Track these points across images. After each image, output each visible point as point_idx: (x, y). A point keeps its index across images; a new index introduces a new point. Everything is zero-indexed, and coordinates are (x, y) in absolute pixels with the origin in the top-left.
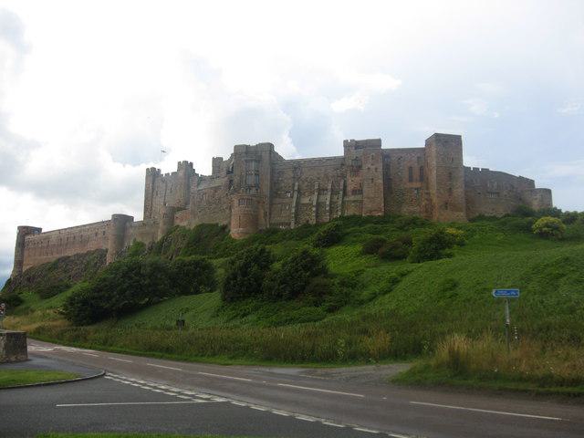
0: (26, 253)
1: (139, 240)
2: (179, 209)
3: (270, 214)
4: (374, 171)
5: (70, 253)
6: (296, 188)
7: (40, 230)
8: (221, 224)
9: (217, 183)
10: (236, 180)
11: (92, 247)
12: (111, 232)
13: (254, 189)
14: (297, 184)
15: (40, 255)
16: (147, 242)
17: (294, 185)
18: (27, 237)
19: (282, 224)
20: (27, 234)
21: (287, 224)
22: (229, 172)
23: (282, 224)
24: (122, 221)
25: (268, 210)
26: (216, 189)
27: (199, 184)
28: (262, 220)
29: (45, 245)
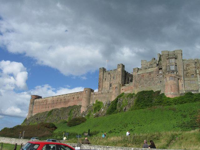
0: (34, 107)
1: (99, 100)
5: (59, 107)
7: (41, 97)
9: (150, 70)
10: (164, 68)
11: (71, 104)
13: (175, 72)
14: (197, 70)
15: (42, 108)
16: (104, 102)
17: (196, 71)
18: (35, 100)
19: (193, 91)
20: (36, 99)
21: (195, 91)
22: (157, 65)
23: (193, 91)
26: (150, 73)
28: (181, 88)
29: (45, 103)
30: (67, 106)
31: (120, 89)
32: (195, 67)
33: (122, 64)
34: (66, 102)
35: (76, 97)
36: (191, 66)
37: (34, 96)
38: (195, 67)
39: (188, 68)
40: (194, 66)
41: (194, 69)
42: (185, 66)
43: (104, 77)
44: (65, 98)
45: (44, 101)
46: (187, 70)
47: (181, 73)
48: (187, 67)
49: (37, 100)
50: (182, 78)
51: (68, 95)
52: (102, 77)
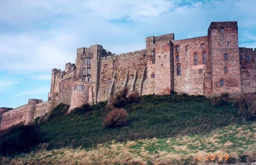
3: (97, 94)
6: (114, 76)
14: (115, 72)
17: (113, 73)
20: (4, 112)
25: (95, 93)
27: (63, 77)
32: (113, 68)
36: (108, 67)
38: (113, 68)
39: (105, 70)
40: (112, 66)
41: (111, 71)
42: (102, 68)
43: (56, 81)
44: (21, 111)
46: (104, 73)
48: (105, 68)
50: (95, 85)
51: (23, 107)
52: (53, 81)
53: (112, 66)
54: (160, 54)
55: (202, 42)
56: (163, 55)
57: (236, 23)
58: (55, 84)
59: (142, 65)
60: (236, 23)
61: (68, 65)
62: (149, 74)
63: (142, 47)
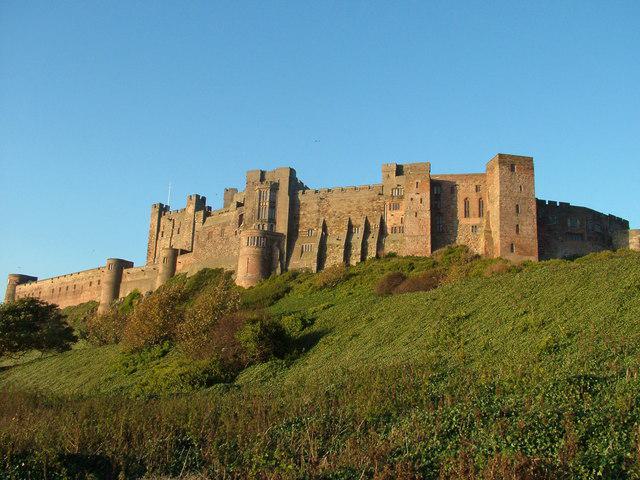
2: (184, 252)
4: (420, 201)
6: (321, 224)
7: (34, 279)
8: (228, 268)
11: (85, 298)
12: (107, 277)
17: (318, 220)
18: (18, 287)
24: (121, 265)
30: (78, 303)
31: (175, 262)
33: (198, 196)
34: (77, 291)
35: (95, 280)
37: (15, 276)
40: (316, 207)
43: (162, 229)
44: (76, 283)
45: (36, 290)
47: (282, 228)
49: (22, 287)
53: (316, 207)
54: (413, 195)
55: (477, 183)
56: (418, 197)
57: (530, 160)
58: (160, 233)
59: (374, 210)
60: (530, 160)
61: (194, 198)
62: (389, 225)
63: (376, 179)
